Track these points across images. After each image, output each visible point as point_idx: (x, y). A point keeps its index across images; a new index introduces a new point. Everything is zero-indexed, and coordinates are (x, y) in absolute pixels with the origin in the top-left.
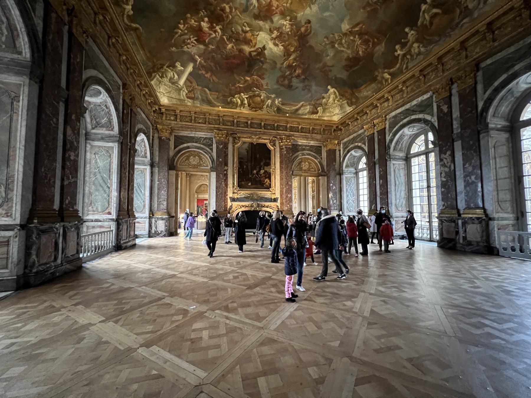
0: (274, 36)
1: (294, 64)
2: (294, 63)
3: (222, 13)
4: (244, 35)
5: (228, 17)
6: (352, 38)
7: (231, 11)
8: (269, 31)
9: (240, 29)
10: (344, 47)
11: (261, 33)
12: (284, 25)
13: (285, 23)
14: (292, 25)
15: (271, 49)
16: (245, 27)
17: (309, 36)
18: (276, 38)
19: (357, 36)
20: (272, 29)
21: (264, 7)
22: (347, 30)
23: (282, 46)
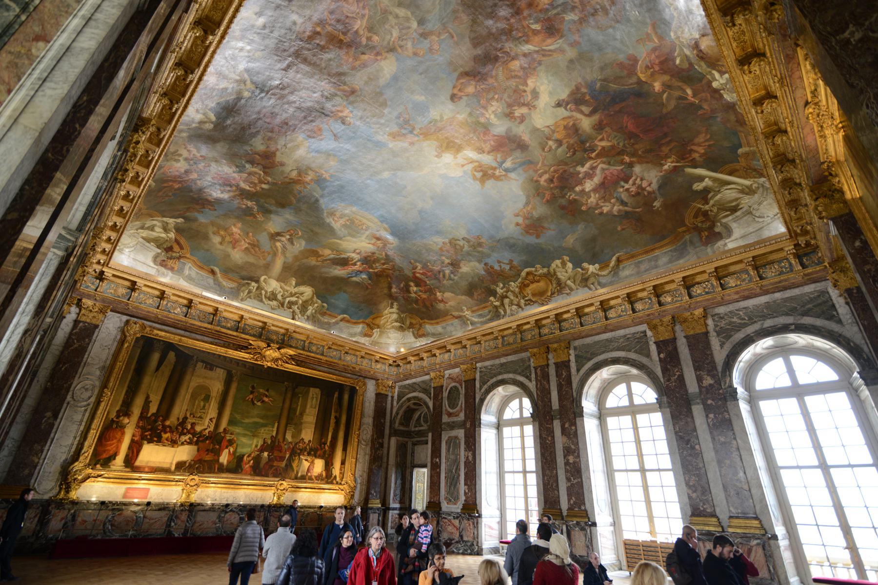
0: (524, 110)
1: (537, 27)
2: (535, 32)
3: (555, 180)
4: (565, 141)
5: (555, 171)
6: (376, 38)
7: (545, 172)
8: (527, 121)
9: (560, 150)
10: (397, 17)
11: (539, 126)
12: (496, 115)
13: (492, 116)
14: (485, 108)
15: (551, 94)
16: (551, 147)
17: (467, 69)
18: (524, 105)
19: (364, 41)
20: (518, 120)
21: (503, 152)
22: (386, 58)
23: (527, 85)
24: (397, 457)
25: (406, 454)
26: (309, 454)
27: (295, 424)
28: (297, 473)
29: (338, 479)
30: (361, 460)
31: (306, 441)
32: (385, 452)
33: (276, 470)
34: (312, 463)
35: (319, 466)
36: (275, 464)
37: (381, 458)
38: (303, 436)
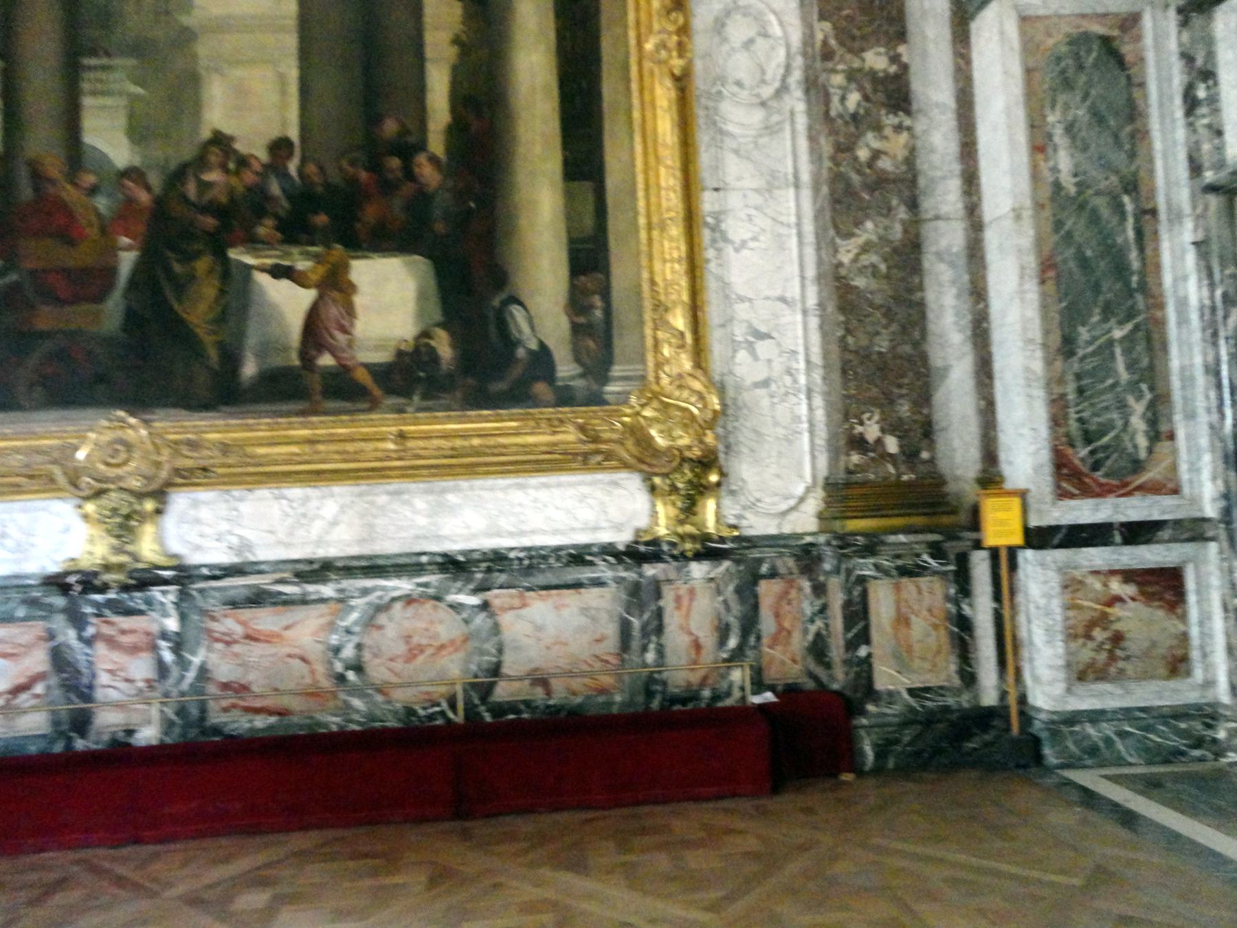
24: (1040, 146)
25: (1133, 113)
26: (294, 230)
27: (139, 49)
28: (231, 360)
29: (566, 369)
30: (736, 229)
31: (253, 141)
32: (939, 138)
33: (60, 355)
34: (335, 285)
35: (389, 300)
36: (46, 318)
37: (906, 185)
38: (217, 114)
